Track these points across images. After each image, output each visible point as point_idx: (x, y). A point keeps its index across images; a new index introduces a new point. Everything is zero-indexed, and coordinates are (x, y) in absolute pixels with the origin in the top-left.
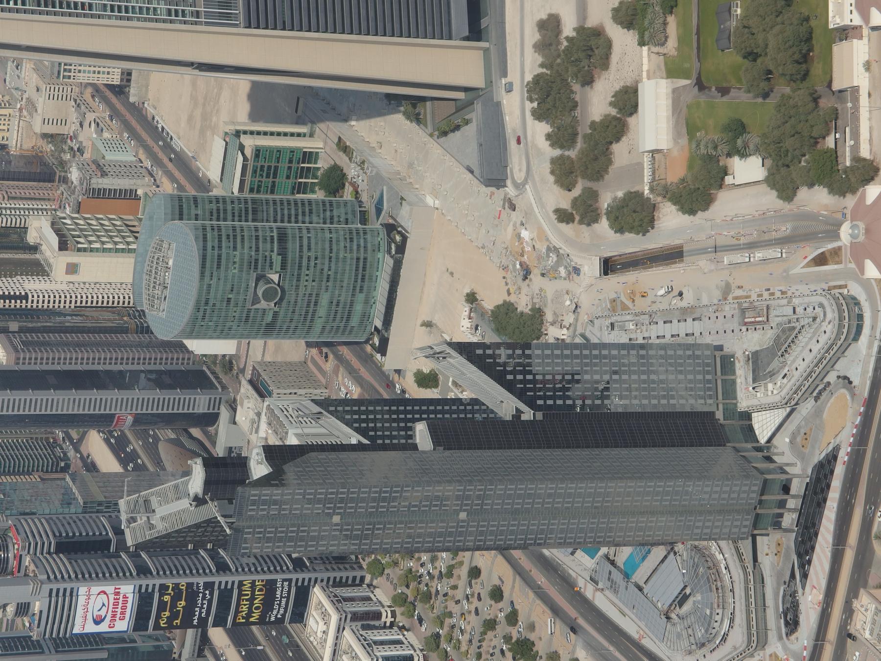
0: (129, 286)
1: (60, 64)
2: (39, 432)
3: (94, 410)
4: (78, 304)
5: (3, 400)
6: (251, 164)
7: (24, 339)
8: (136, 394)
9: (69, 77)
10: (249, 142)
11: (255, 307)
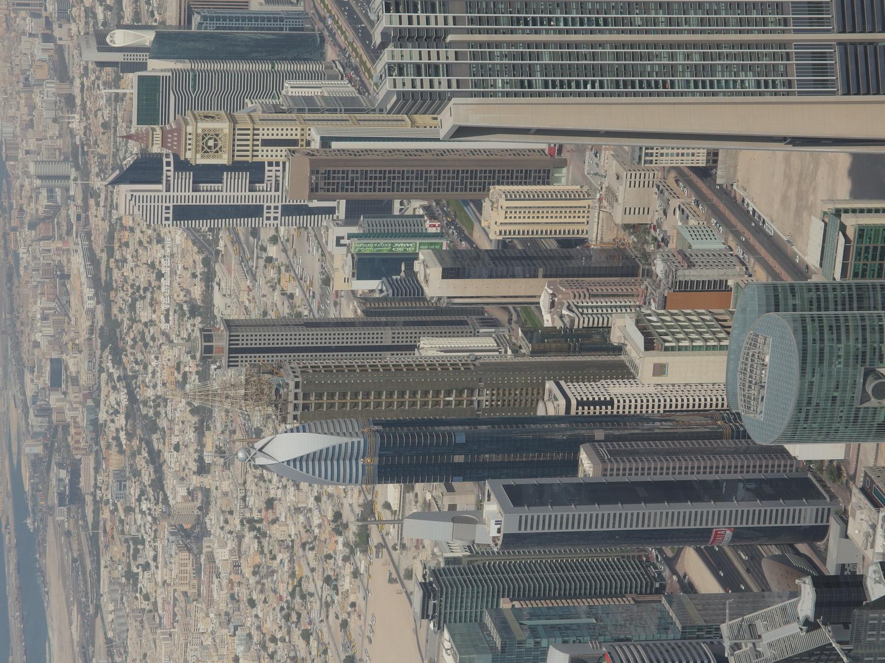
0: (722, 387)
1: (641, 148)
2: (631, 550)
4: (668, 408)
6: (853, 246)
8: (734, 506)
9: (651, 162)
10: (851, 222)
11: (866, 405)
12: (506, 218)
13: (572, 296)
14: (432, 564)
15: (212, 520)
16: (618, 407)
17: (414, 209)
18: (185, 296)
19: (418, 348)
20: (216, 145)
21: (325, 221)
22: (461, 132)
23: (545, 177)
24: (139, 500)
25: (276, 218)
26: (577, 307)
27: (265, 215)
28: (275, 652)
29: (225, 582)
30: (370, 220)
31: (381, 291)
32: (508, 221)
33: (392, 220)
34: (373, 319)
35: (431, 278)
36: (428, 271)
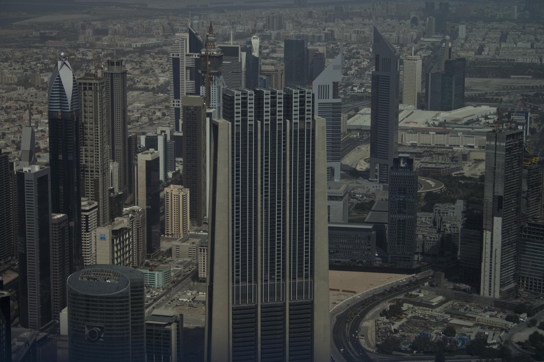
0: (94, 263)
1: (207, 247)
3: (30, 301)
4: (85, 258)
5: (32, 181)
7: (66, 228)
9: (201, 252)
11: (86, 327)
12: (174, 195)
13: (138, 220)
14: (10, 156)
15: (33, 90)
16: (85, 235)
17: (178, 167)
18: (138, 81)
19: (113, 161)
22: (215, 127)
24: (42, 63)
26: (132, 221)
27: (175, 100)
29: (3, 95)
30: (173, 145)
31: (140, 147)
32: (173, 196)
33: (173, 158)
35: (146, 155)
36: (149, 154)
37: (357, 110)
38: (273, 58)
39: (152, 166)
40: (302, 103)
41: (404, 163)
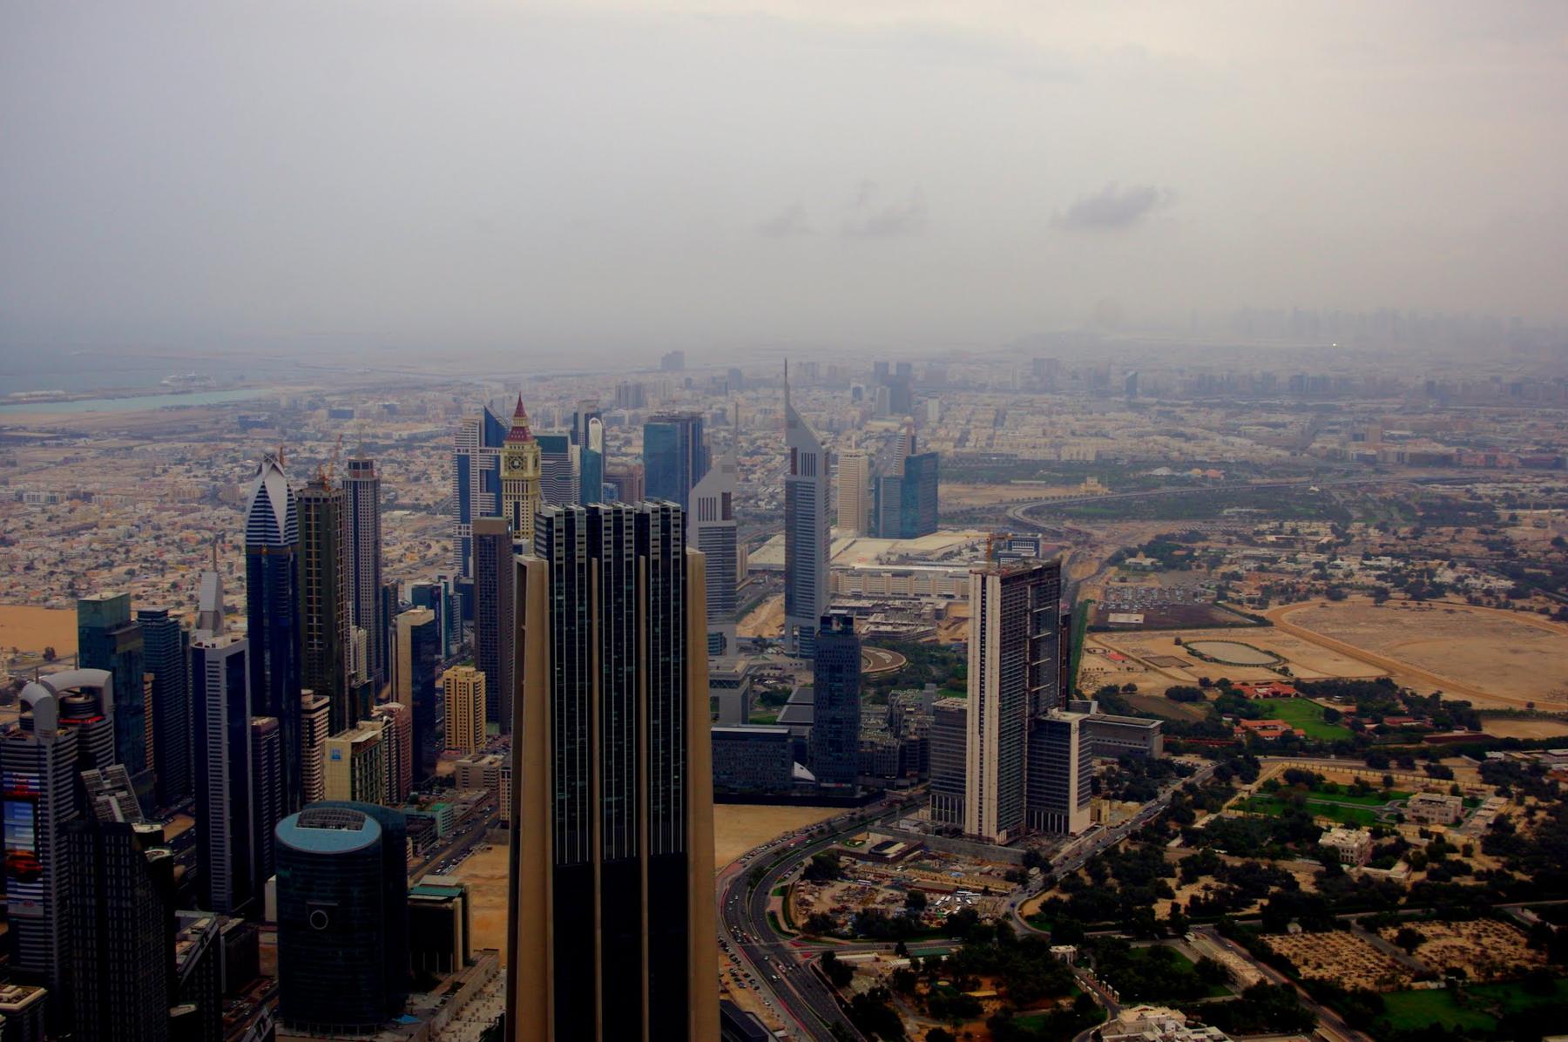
9: (503, 777)
14: (182, 622)
15: (225, 512)
20: (514, 467)
21: (457, 569)
23: (490, 719)
24: (242, 466)
25: (460, 533)
28: (118, 553)
29: (176, 519)
34: (381, 595)
37: (764, 540)
38: (626, 455)
39: (423, 638)
40: (666, 528)
41: (838, 625)
